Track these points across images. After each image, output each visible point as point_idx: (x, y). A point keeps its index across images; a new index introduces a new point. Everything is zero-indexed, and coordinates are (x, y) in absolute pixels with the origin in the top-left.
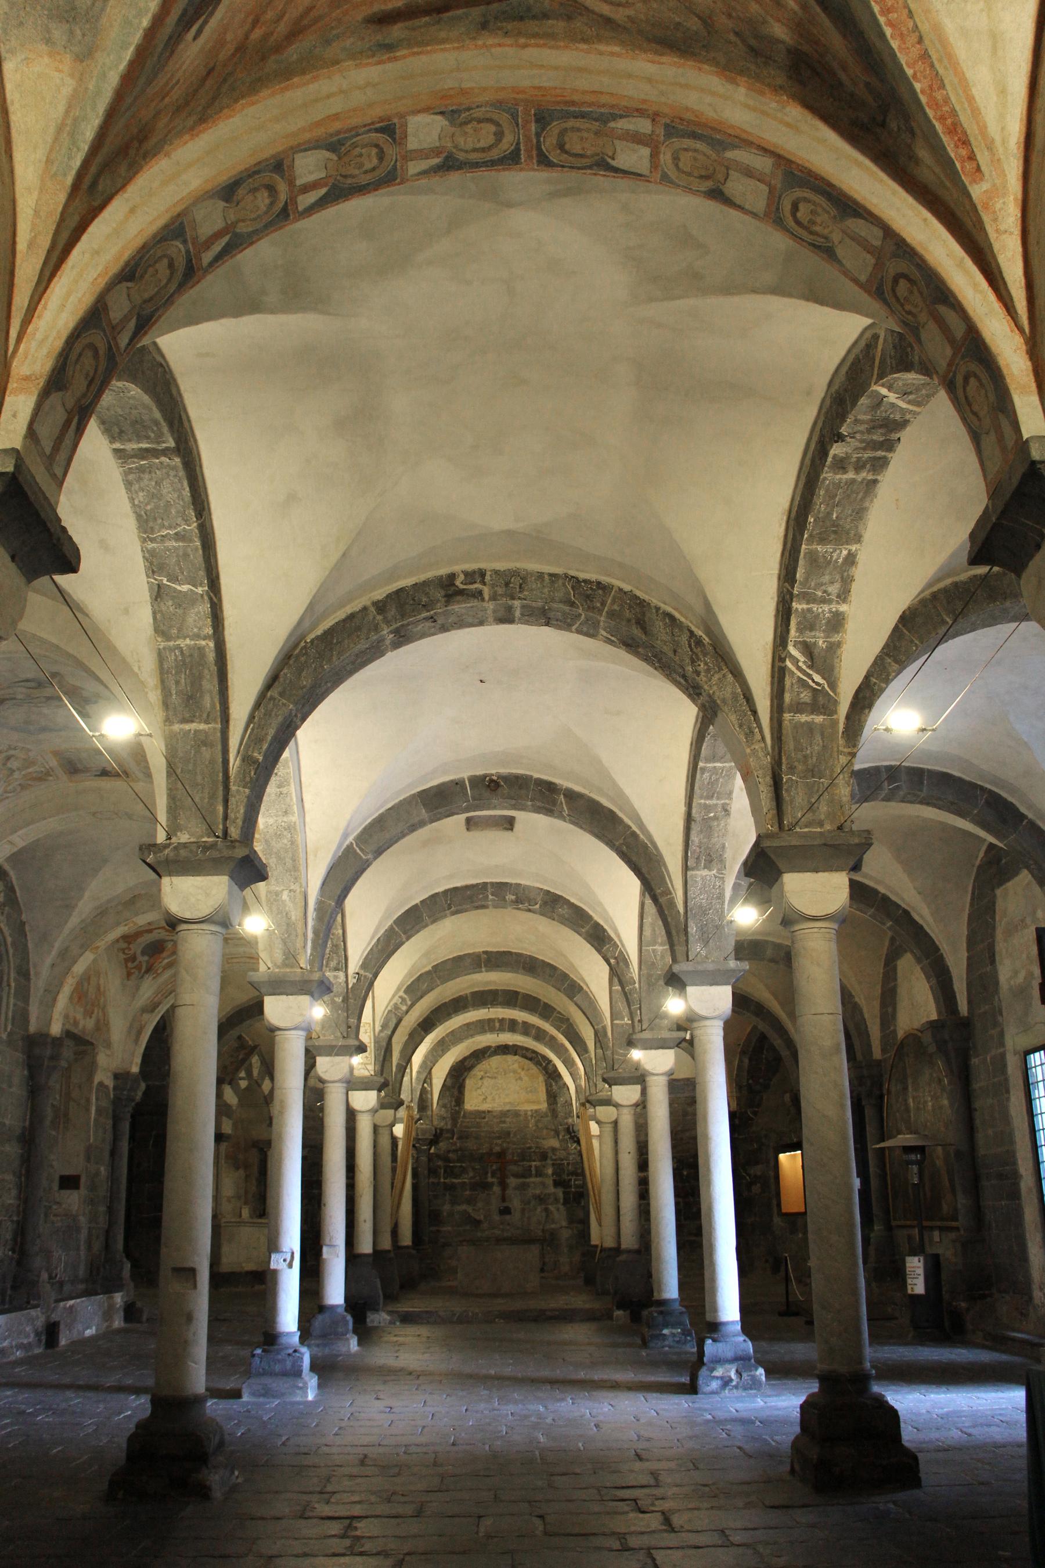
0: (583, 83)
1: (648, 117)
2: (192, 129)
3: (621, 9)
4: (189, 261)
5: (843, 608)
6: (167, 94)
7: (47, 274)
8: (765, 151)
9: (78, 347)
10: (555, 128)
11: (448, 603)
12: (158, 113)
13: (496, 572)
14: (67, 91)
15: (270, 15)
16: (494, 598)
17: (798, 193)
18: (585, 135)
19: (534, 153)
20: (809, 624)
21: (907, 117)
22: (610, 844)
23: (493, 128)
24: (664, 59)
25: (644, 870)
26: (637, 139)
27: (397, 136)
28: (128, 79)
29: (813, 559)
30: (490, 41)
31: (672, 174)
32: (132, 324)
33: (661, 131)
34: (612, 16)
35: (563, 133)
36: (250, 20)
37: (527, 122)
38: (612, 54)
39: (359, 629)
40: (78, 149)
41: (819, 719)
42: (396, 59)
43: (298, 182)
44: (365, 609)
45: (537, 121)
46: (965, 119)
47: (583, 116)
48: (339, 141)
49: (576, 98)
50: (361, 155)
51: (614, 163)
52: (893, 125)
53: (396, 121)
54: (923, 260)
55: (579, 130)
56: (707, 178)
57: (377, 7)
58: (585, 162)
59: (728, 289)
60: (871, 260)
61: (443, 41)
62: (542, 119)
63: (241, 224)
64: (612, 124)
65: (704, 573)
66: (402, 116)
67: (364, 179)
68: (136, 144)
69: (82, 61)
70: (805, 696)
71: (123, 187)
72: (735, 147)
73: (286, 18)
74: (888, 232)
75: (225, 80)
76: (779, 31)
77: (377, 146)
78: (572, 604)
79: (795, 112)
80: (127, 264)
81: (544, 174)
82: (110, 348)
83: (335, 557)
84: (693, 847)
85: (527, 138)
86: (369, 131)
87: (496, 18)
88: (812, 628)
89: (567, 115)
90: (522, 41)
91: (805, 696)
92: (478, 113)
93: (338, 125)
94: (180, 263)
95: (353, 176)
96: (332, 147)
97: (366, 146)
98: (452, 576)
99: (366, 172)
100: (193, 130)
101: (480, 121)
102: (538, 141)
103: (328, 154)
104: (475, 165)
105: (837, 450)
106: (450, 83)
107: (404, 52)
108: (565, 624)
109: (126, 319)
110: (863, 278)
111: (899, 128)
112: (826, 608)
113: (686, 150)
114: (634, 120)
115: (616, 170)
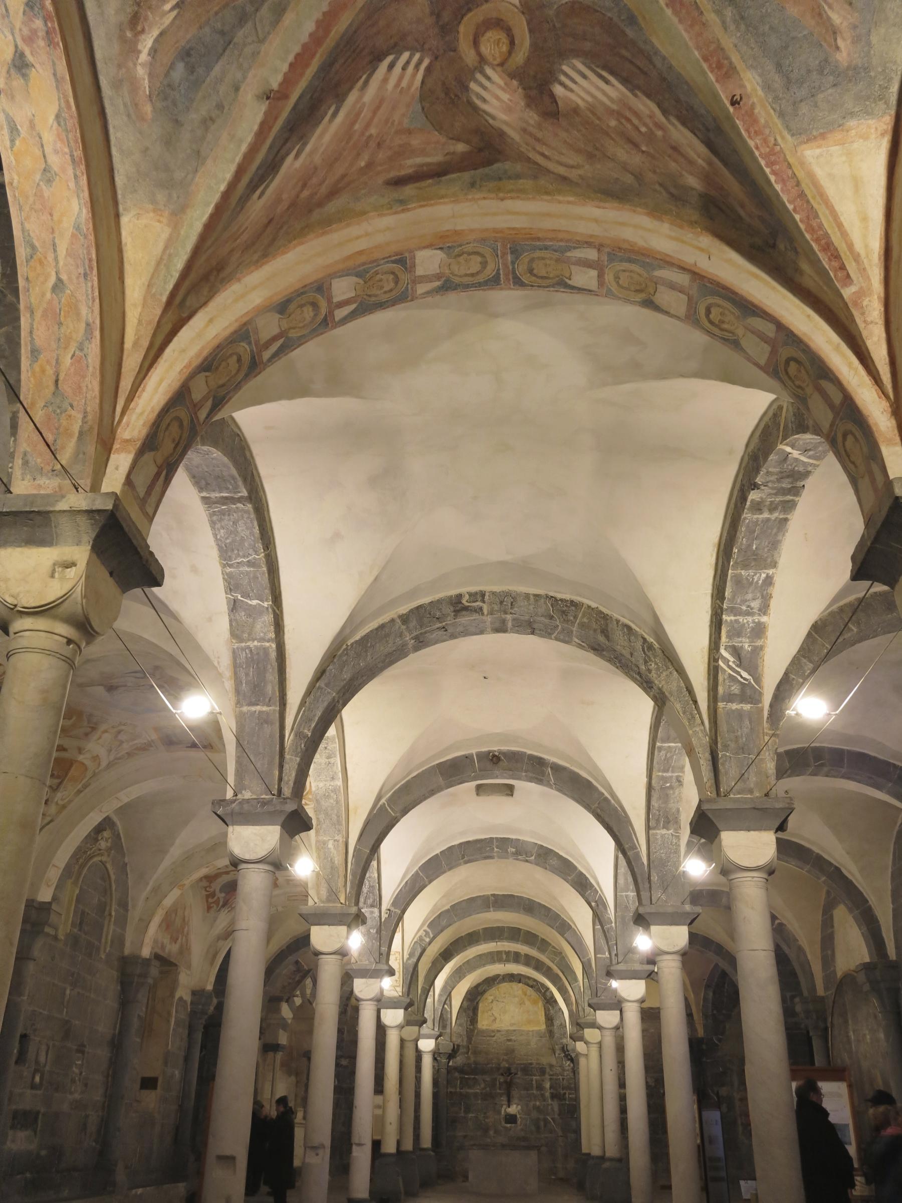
0: (549, 224)
1: (595, 247)
2: (257, 261)
3: (573, 170)
4: (253, 358)
5: (764, 619)
7: (146, 364)
8: (683, 269)
9: (167, 420)
10: (525, 258)
11: (456, 616)
12: (232, 251)
13: (493, 593)
14: (165, 236)
15: (314, 180)
16: (491, 613)
17: (710, 300)
18: (548, 262)
19: (511, 277)
20: (737, 632)
21: (791, 240)
22: (588, 807)
23: (479, 259)
24: (607, 205)
25: (615, 829)
26: (586, 264)
27: (408, 266)
28: (209, 227)
29: (738, 581)
30: (477, 196)
32: (209, 403)
34: (566, 174)
35: (532, 260)
36: (300, 184)
37: (504, 254)
38: (569, 202)
39: (387, 635)
40: (172, 276)
41: (747, 707)
42: (408, 210)
43: (335, 300)
44: (393, 620)
45: (512, 253)
46: (836, 239)
47: (546, 248)
48: (364, 270)
49: (540, 235)
50: (381, 280)
52: (781, 246)
53: (407, 255)
54: (807, 346)
55: (543, 259)
57: (393, 174)
58: (548, 282)
59: (663, 375)
60: (767, 348)
61: (443, 197)
62: (516, 252)
63: (292, 331)
64: (569, 254)
65: (654, 593)
66: (411, 251)
67: (384, 298)
68: (215, 273)
69: (176, 215)
70: (735, 689)
71: (205, 303)
72: (660, 268)
73: (327, 182)
74: (780, 326)
75: (281, 228)
76: (692, 181)
77: (393, 273)
78: (551, 617)
79: (707, 240)
80: (206, 359)
81: (519, 293)
82: (192, 420)
83: (371, 579)
84: (654, 811)
85: (505, 265)
86: (388, 262)
87: (481, 179)
88: (739, 635)
89: (534, 248)
90: (501, 195)
91: (735, 689)
92: (469, 248)
93: (363, 259)
94: (246, 359)
95: (376, 296)
96: (358, 275)
97: (385, 273)
98: (460, 596)
99: (385, 292)
100: (258, 263)
101: (469, 254)
102: (513, 268)
103: (354, 279)
104: (466, 287)
105: (753, 496)
106: (448, 226)
107: (414, 205)
108: (547, 633)
109: (205, 399)
110: (762, 362)
111: (786, 248)
112: (750, 619)
113: (624, 271)
114: (585, 250)
115: (573, 288)
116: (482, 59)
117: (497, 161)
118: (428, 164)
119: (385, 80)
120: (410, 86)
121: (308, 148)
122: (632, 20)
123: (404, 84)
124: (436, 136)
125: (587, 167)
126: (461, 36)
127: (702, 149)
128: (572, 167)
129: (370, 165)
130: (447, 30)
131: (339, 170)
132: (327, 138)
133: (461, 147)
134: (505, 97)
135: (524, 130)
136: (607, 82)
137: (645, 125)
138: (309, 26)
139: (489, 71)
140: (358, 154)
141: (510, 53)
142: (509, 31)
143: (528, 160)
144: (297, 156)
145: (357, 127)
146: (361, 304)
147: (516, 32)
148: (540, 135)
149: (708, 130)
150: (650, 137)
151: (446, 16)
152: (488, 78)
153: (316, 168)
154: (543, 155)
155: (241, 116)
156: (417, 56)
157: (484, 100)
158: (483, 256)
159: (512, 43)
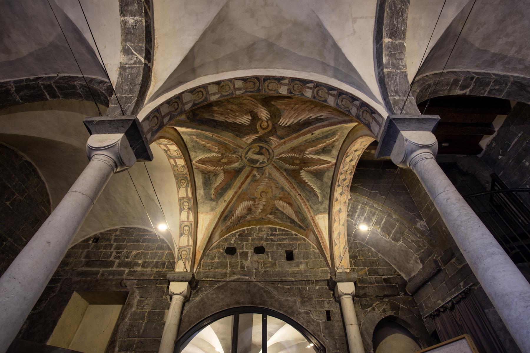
6: (331, 112)
10: (256, 88)
15: (309, 108)
18: (249, 87)
23: (269, 88)
26: (239, 89)
27: (289, 91)
31: (230, 83)
33: (234, 93)
35: (254, 87)
37: (262, 89)
45: (260, 89)
51: (243, 82)
55: (251, 88)
56: (222, 87)
57: (290, 100)
63: (326, 92)
64: (244, 91)
67: (298, 83)
77: (294, 90)
85: (262, 86)
86: (295, 94)
95: (300, 84)
99: (297, 84)
101: (272, 90)
102: (259, 84)
103: (304, 94)
113: (228, 91)
114: (240, 93)
116: (267, 122)
117: (264, 98)
118: (281, 100)
119: (288, 122)
120: (283, 119)
121: (308, 117)
122: (237, 135)
123: (284, 120)
124: (279, 107)
125: (241, 100)
126: (271, 127)
127: (216, 119)
128: (245, 99)
129: (296, 104)
130: (274, 128)
131: (303, 107)
132: (304, 116)
133: (273, 103)
134: (262, 114)
135: (257, 107)
136: (240, 122)
137: (230, 116)
138: (300, 138)
139: (266, 120)
140: (298, 108)
141: (261, 124)
142: (261, 128)
143: (256, 99)
144: (311, 117)
145: (296, 115)
146: (305, 85)
147: (260, 128)
148: (254, 106)
149: (217, 124)
150: (228, 114)
151: (274, 130)
152: (266, 118)
153: (308, 111)
154: (253, 101)
155: (318, 134)
156: (281, 124)
157: (267, 113)
158: (268, 89)
159: (261, 126)
